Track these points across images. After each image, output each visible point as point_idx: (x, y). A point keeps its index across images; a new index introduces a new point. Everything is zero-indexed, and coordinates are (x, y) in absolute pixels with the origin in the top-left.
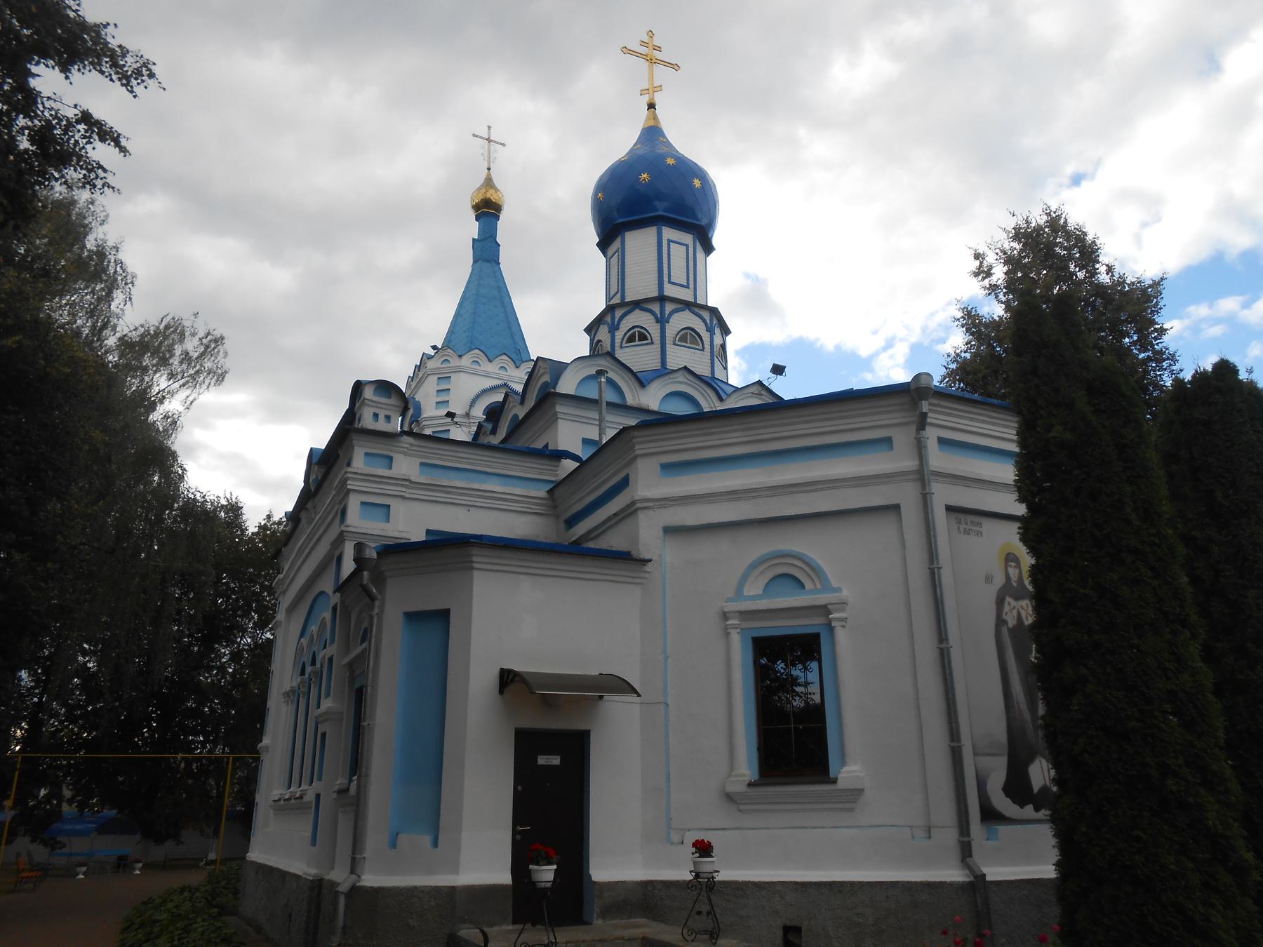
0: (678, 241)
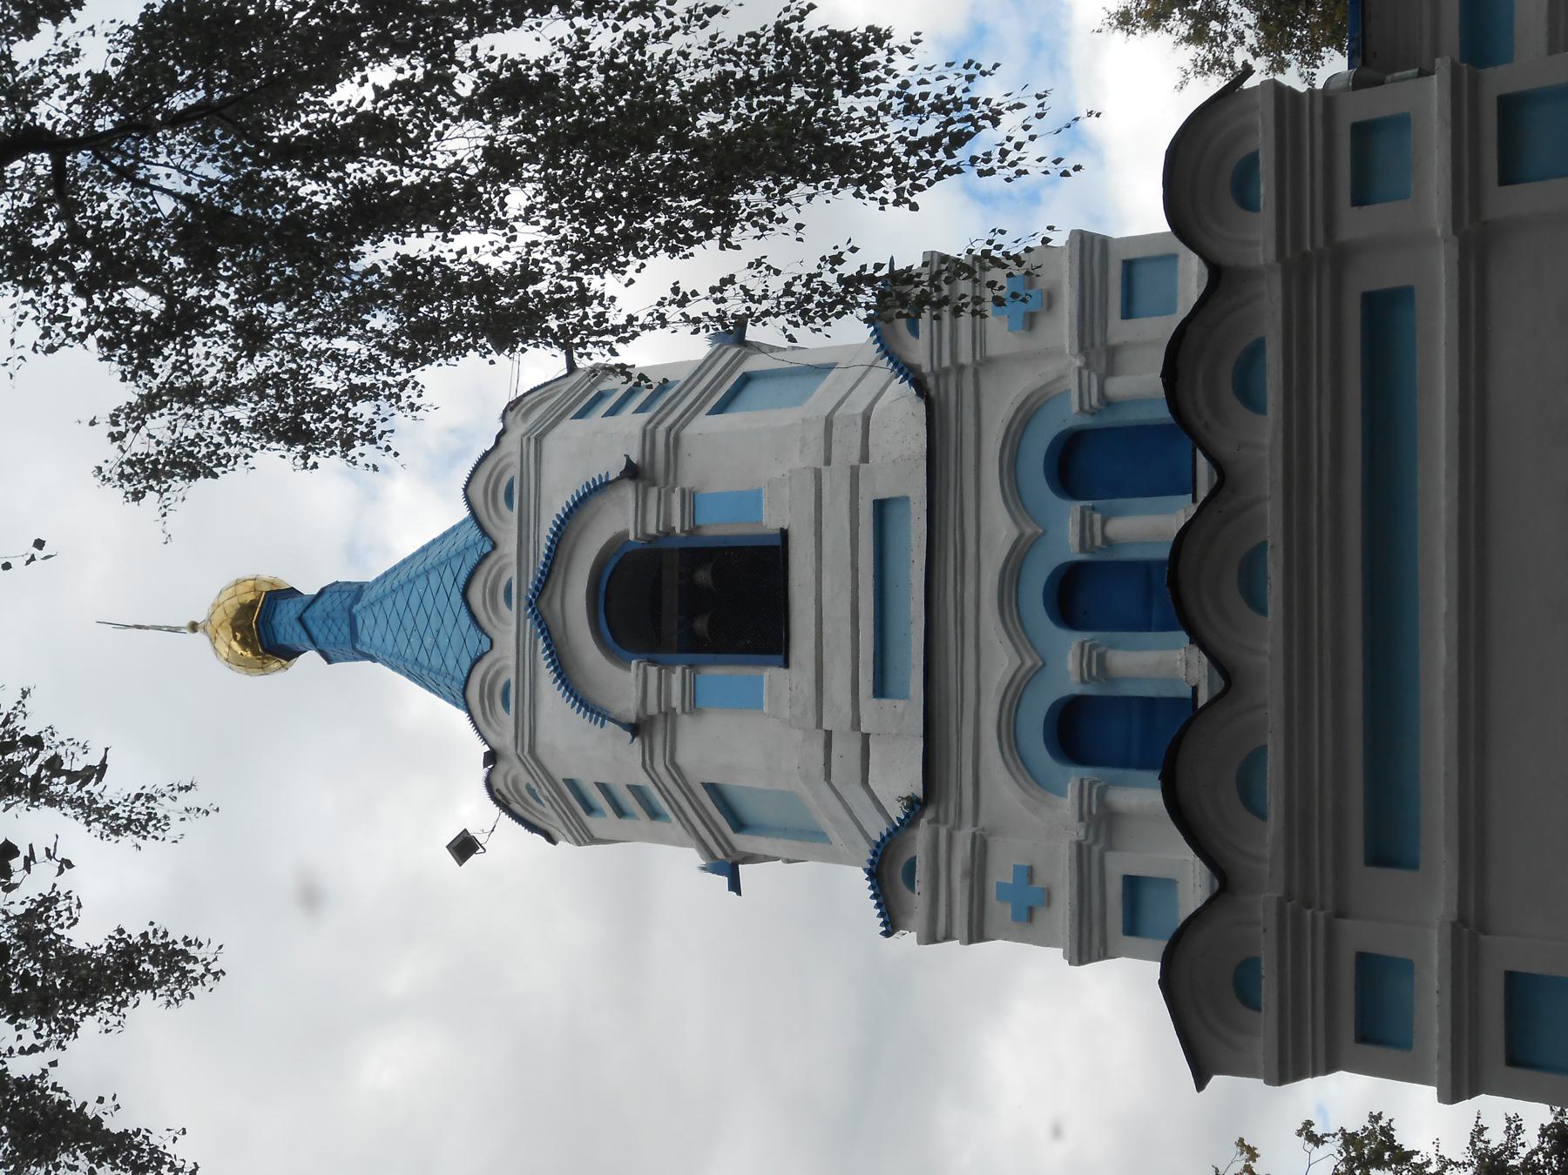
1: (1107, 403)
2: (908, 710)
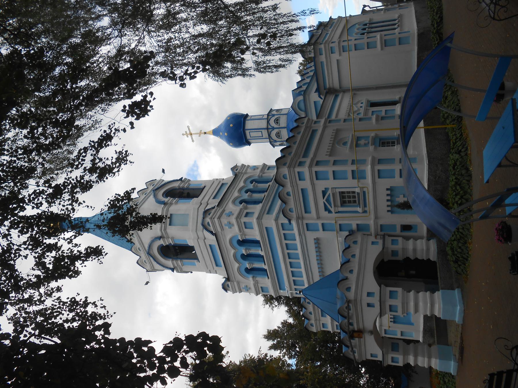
0: (249, 125)
1: (262, 176)
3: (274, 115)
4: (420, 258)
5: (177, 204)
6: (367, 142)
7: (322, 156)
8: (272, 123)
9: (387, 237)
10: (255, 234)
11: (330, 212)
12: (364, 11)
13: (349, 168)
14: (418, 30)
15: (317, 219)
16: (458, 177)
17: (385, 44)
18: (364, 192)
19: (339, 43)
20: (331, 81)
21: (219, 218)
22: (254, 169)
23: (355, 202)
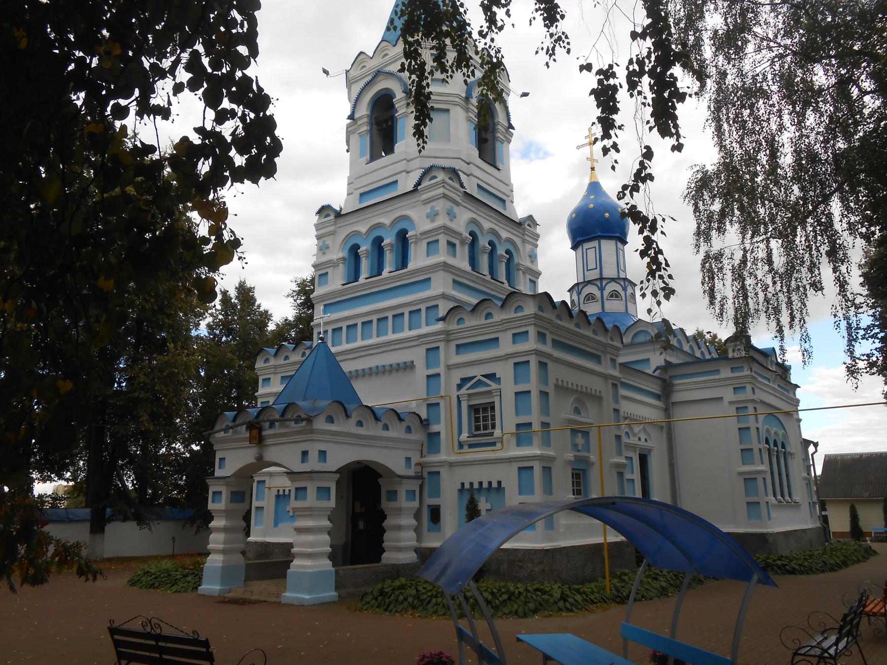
0: (608, 247)
1: (519, 270)
2: (476, 193)
3: (625, 289)
4: (386, 536)
5: (467, 121)
6: (580, 448)
7: (555, 373)
8: (612, 287)
9: (419, 482)
10: (418, 259)
11: (460, 387)
12: (807, 443)
13: (535, 418)
14: (772, 534)
15: (448, 366)
16: (522, 597)
17: (749, 480)
18: (494, 444)
19: (753, 401)
20: (688, 387)
21: (445, 196)
22: (530, 256)
23: (478, 428)
